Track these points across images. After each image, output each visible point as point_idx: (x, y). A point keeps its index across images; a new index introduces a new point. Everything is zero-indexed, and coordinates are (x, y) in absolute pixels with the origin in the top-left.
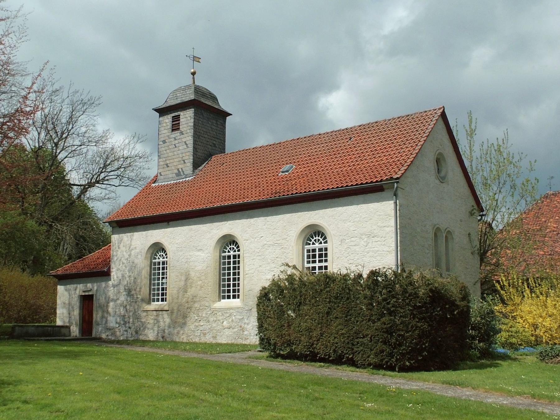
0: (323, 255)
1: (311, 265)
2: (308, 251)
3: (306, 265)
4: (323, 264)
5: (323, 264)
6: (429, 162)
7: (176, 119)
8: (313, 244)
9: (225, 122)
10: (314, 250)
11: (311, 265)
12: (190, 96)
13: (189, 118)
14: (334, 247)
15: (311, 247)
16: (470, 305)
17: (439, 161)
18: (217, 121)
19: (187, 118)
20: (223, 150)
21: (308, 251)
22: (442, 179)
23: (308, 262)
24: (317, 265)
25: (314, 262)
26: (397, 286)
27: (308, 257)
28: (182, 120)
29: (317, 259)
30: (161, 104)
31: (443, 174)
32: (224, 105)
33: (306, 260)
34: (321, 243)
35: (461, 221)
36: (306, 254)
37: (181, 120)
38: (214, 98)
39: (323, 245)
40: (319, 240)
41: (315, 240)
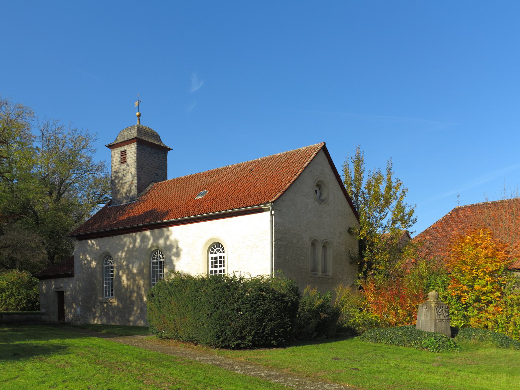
0: (221, 261)
1: (214, 269)
2: (212, 258)
3: (210, 269)
4: (222, 268)
5: (222, 268)
6: (308, 186)
7: (124, 153)
8: (216, 253)
9: (166, 156)
10: (216, 258)
11: (214, 269)
12: (134, 134)
13: (133, 153)
14: (229, 256)
15: (214, 255)
16: (217, 349)
17: (319, 186)
18: (158, 155)
19: (132, 150)
20: (166, 178)
21: (212, 258)
22: (321, 201)
23: (212, 267)
24: (218, 269)
25: (216, 267)
26: (142, 322)
27: (212, 263)
28: (128, 154)
29: (218, 265)
30: (111, 142)
31: (323, 197)
32: (166, 142)
33: (210, 265)
34: (221, 252)
35: (340, 233)
36: (210, 261)
37: (128, 155)
38: (157, 137)
39: (222, 255)
40: (219, 250)
41: (217, 250)
